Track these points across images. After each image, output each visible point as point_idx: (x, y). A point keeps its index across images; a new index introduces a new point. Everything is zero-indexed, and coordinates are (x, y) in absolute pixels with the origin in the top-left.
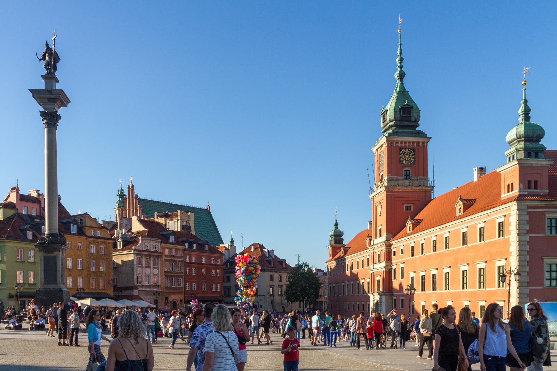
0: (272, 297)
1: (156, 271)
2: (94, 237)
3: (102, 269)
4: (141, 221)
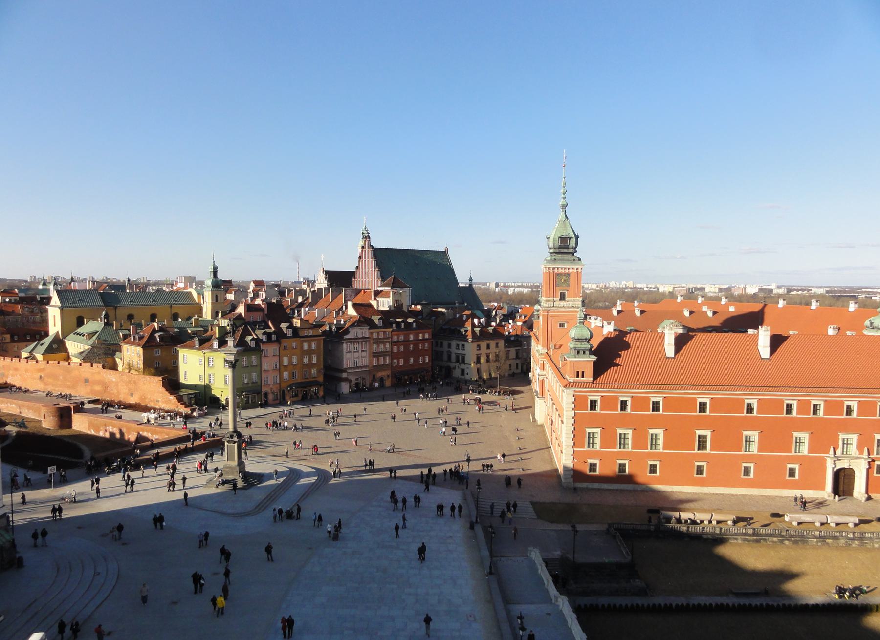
0: (478, 366)
1: (364, 354)
2: (306, 337)
3: (314, 361)
4: (355, 306)
